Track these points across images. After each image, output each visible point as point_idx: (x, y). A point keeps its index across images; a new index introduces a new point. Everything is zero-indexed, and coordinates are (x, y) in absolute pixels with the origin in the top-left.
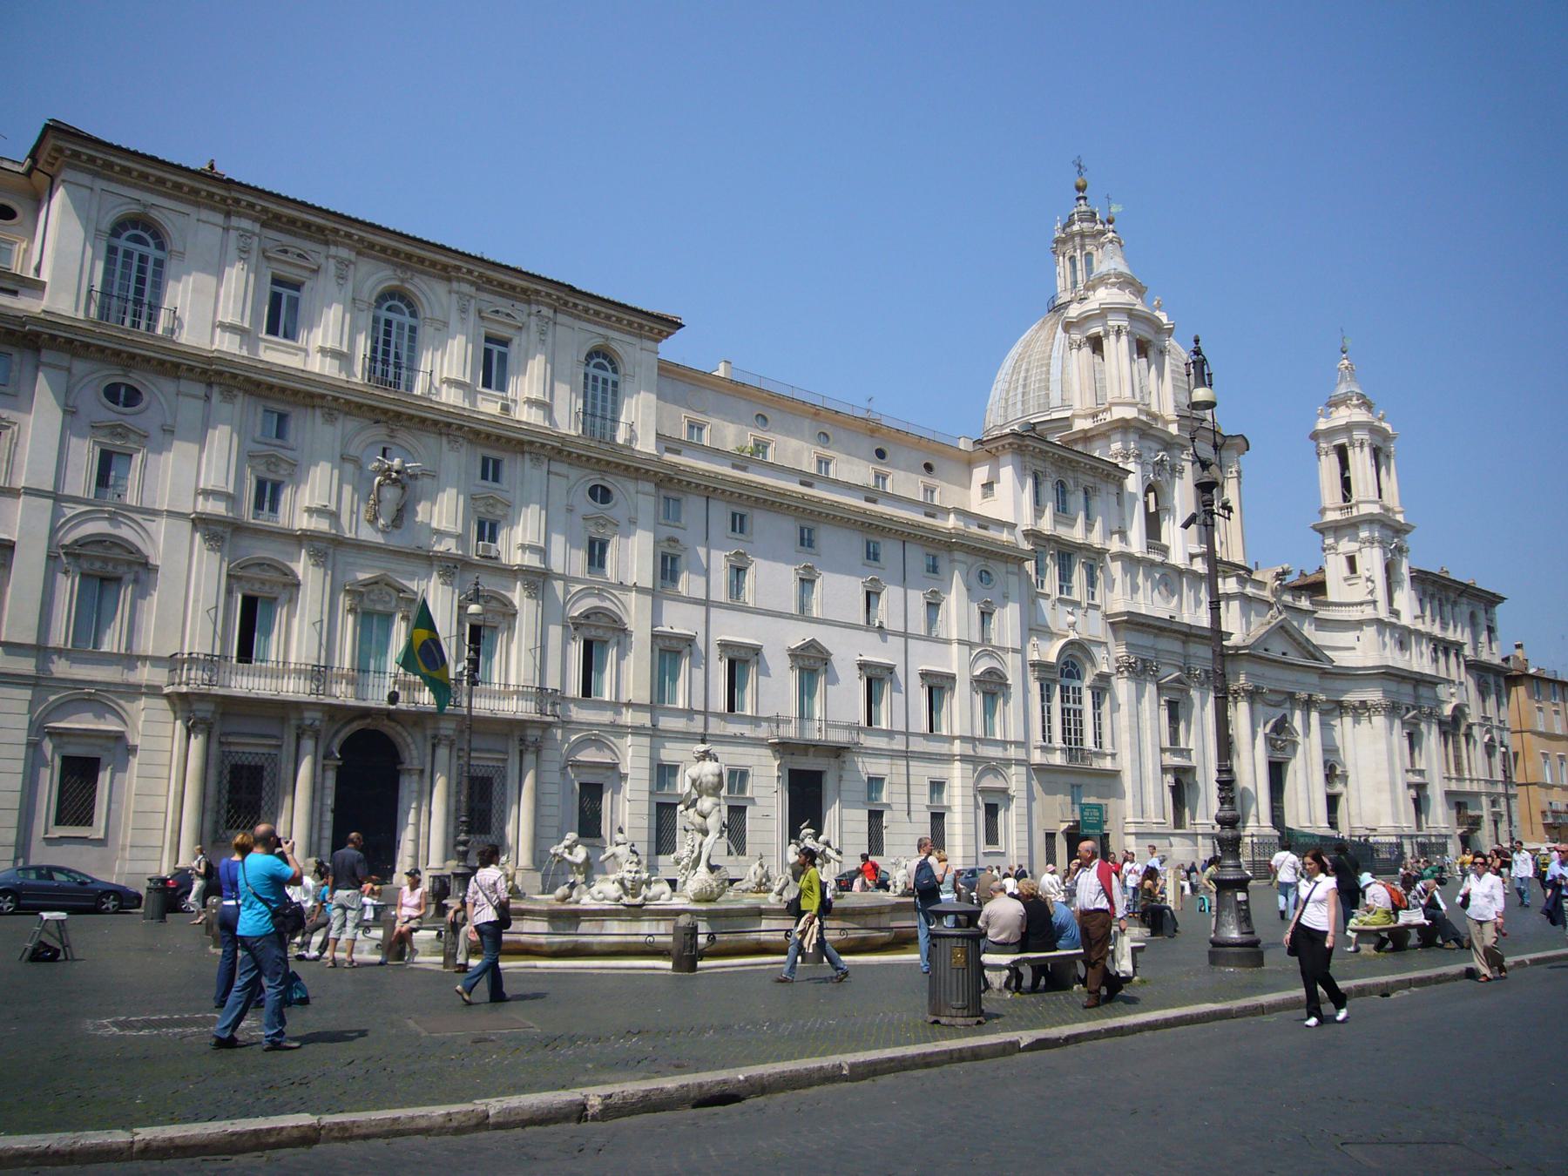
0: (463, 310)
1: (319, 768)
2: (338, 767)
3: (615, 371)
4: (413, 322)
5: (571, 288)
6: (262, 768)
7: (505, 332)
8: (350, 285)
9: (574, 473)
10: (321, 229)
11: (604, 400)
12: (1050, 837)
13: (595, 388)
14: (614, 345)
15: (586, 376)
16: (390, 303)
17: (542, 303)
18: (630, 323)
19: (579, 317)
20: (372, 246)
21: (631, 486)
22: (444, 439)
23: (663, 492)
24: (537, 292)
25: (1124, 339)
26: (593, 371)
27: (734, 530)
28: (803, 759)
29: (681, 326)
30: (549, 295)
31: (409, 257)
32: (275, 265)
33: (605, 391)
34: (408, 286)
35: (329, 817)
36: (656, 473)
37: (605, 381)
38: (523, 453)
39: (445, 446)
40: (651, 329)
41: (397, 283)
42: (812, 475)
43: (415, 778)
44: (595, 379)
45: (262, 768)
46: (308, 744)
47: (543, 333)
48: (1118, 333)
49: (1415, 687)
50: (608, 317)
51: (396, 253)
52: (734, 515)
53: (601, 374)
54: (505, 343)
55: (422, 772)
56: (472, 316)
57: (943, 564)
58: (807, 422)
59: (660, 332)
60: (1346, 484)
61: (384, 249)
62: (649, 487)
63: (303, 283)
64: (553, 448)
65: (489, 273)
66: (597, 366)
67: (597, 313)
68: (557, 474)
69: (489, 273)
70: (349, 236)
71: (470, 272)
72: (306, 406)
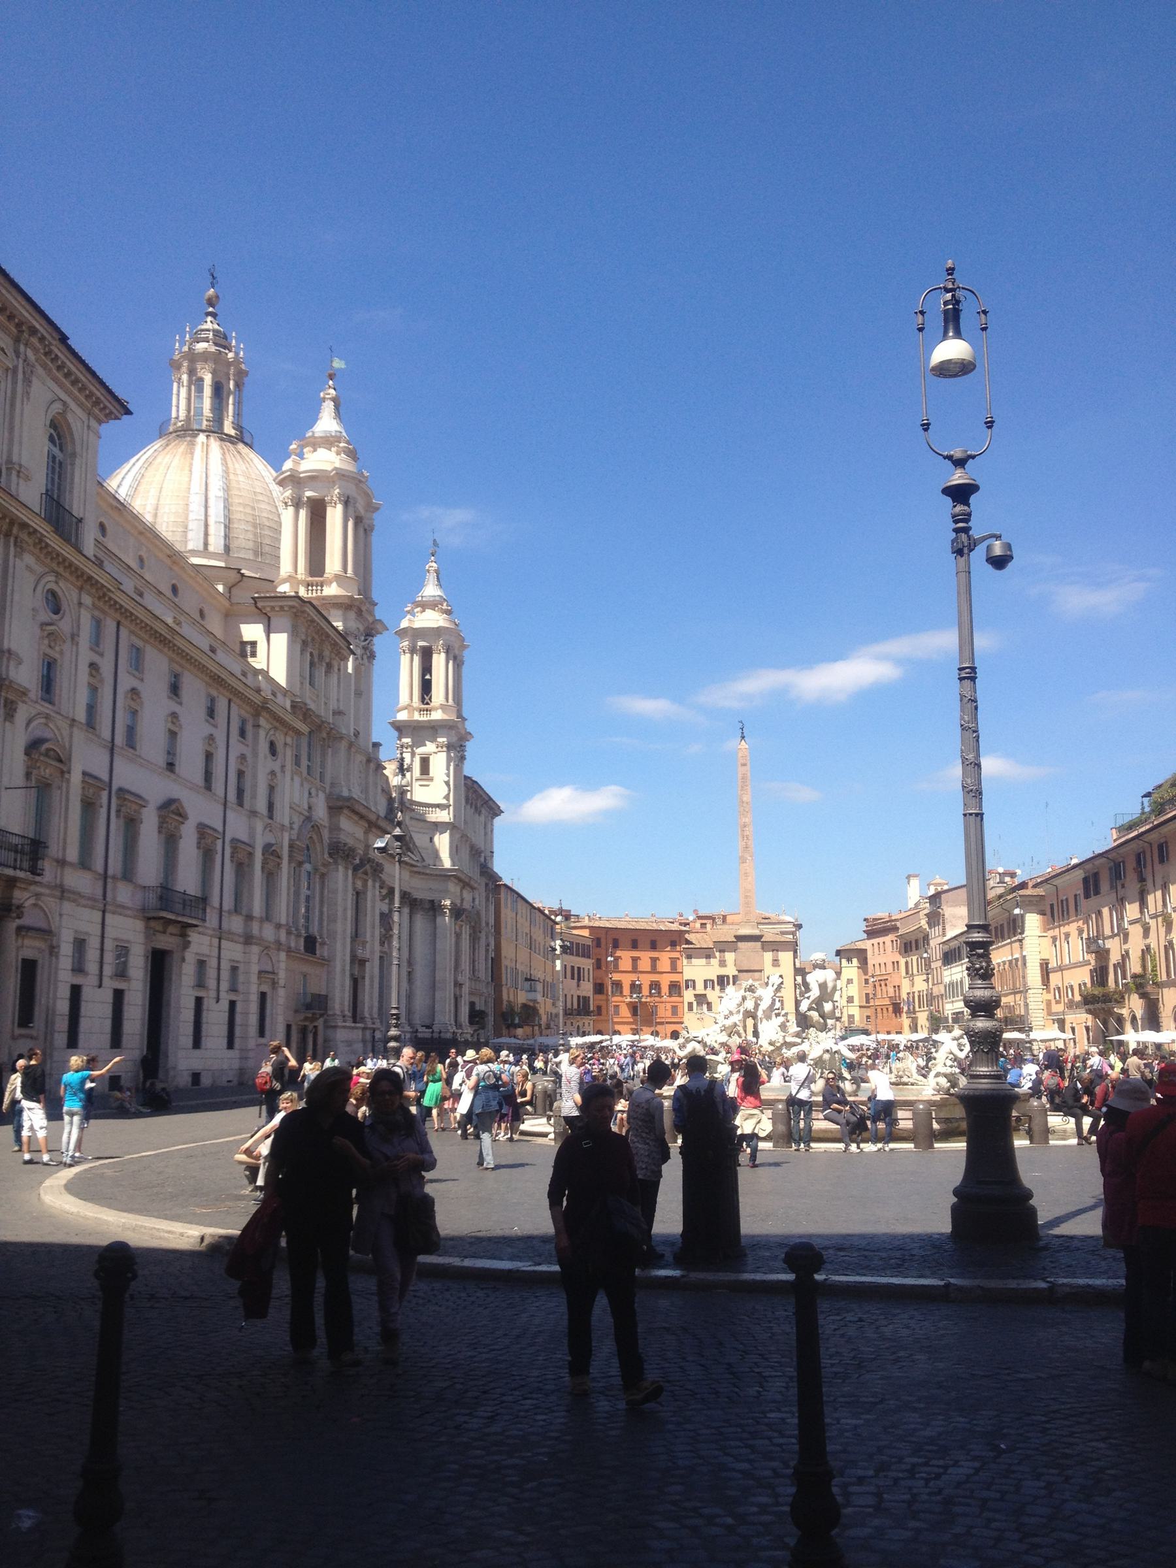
5: (64, 339)
12: (289, 1027)
14: (70, 417)
24: (33, 331)
28: (161, 937)
29: (128, 412)
30: (42, 339)
49: (463, 888)
60: (426, 687)
62: (87, 600)
67: (68, 375)
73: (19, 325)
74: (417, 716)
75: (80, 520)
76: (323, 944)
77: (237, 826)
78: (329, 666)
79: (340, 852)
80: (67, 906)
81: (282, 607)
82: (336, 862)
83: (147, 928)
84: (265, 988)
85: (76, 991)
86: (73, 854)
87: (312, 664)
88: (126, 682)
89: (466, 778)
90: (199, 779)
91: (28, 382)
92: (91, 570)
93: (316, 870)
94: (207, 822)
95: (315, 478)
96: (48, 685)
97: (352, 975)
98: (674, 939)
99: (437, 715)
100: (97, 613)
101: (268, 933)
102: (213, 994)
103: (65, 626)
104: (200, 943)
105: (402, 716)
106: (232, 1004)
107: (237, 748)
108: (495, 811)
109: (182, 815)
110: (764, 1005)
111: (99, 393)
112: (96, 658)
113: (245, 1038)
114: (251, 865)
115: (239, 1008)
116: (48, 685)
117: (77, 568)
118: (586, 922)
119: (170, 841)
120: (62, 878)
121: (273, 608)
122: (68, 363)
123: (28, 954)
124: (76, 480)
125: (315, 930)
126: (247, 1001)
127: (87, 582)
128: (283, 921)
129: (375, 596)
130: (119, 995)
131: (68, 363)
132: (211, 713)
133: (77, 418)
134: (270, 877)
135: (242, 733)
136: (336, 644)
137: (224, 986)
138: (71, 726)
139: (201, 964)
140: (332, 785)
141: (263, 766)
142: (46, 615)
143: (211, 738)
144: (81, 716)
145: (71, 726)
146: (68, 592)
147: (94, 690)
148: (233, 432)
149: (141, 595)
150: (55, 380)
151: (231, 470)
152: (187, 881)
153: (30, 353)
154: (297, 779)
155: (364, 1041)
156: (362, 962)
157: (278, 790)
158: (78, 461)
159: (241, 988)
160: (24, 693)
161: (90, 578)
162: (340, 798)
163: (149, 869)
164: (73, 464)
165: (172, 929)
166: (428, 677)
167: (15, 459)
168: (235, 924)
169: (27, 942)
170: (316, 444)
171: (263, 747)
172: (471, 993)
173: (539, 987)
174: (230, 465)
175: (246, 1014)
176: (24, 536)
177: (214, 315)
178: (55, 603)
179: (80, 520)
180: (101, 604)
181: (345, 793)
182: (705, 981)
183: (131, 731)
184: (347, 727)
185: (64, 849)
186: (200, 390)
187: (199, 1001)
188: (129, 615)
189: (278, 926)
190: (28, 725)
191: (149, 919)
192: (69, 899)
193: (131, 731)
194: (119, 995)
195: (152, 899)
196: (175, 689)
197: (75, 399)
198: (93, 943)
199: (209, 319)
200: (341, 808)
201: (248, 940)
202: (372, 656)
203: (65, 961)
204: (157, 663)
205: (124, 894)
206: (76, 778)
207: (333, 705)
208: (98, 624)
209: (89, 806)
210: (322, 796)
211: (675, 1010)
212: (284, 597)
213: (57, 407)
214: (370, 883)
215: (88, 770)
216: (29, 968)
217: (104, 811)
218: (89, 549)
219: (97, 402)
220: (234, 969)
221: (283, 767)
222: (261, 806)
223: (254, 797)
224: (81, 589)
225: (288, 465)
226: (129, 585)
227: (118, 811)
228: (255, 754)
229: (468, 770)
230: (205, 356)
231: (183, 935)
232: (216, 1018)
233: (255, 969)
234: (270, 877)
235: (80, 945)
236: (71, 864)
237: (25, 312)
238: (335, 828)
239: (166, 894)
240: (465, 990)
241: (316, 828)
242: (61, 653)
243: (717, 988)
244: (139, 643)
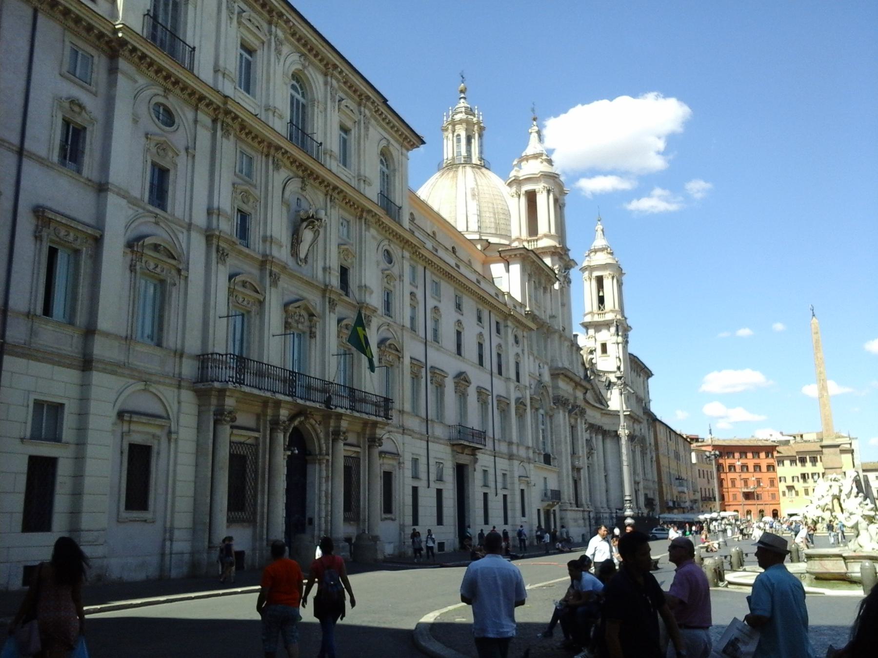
5: (385, 101)
7: (349, 124)
12: (539, 510)
14: (391, 148)
24: (368, 98)
25: (551, 196)
29: (423, 143)
30: (373, 102)
38: (361, 218)
41: (300, 67)
48: (549, 191)
60: (601, 300)
62: (407, 254)
70: (287, 21)
73: (360, 96)
74: (596, 318)
75: (400, 208)
76: (555, 458)
77: (499, 387)
78: (545, 289)
79: (560, 402)
80: (407, 438)
81: (515, 255)
82: (558, 408)
83: (453, 451)
84: (523, 487)
85: (415, 490)
86: (408, 407)
87: (535, 288)
88: (431, 303)
89: (630, 354)
90: (476, 360)
92: (407, 236)
93: (547, 413)
94: (481, 385)
95: (529, 180)
96: (388, 305)
97: (573, 477)
98: (769, 450)
99: (609, 316)
100: (412, 262)
101: (522, 452)
102: (493, 491)
103: (395, 270)
104: (484, 460)
105: (588, 319)
106: (505, 496)
107: (496, 340)
108: (649, 374)
109: (467, 381)
110: (846, 490)
111: (407, 133)
112: (414, 290)
113: (514, 517)
115: (509, 499)
116: (388, 305)
117: (400, 236)
118: (709, 442)
119: (462, 396)
123: (387, 468)
124: (397, 184)
125: (549, 450)
126: (513, 494)
127: (406, 243)
128: (530, 445)
129: (569, 245)
130: (439, 492)
132: (480, 319)
133: (395, 149)
134: (521, 416)
135: (498, 331)
136: (548, 275)
137: (500, 486)
138: (402, 330)
139: (485, 471)
140: (552, 361)
141: (511, 351)
142: (384, 265)
143: (481, 334)
144: (408, 324)
146: (396, 250)
147: (413, 308)
148: (479, 163)
149: (436, 251)
150: (381, 126)
151: (479, 184)
152: (474, 421)
153: (367, 112)
154: (531, 358)
155: (584, 519)
156: (579, 470)
157: (521, 365)
158: (397, 173)
159: (509, 486)
160: (375, 311)
161: (408, 241)
162: (557, 368)
163: (451, 415)
164: (394, 176)
165: (466, 451)
166: (601, 294)
167: (362, 173)
168: (503, 448)
169: (386, 461)
170: (527, 158)
171: (511, 339)
172: (644, 488)
173: (685, 484)
174: (478, 181)
175: (513, 502)
176: (369, 218)
177: (465, 98)
178: (389, 257)
179: (400, 208)
180: (415, 257)
181: (560, 365)
182: (793, 477)
183: (435, 331)
184: (558, 325)
186: (459, 141)
187: (485, 495)
188: (430, 263)
189: (528, 448)
190: (378, 330)
191: (453, 445)
192: (406, 434)
193: (435, 331)
194: (439, 492)
195: (454, 433)
196: (459, 307)
197: (393, 137)
198: (423, 461)
199: (462, 100)
200: (558, 374)
201: (511, 457)
202: (569, 282)
203: (408, 473)
204: (448, 290)
206: (407, 361)
207: (549, 312)
208: (413, 269)
209: (415, 377)
210: (546, 367)
211: (774, 496)
212: (517, 249)
213: (384, 143)
214: (579, 420)
215: (413, 356)
216: (388, 477)
217: (423, 380)
218: (406, 223)
219: (406, 138)
220: (504, 475)
221: (523, 350)
222: (513, 376)
223: (508, 369)
224: (403, 248)
225: (513, 174)
226: (429, 245)
227: (431, 380)
228: (507, 343)
229: (631, 349)
230: (461, 122)
231: (474, 455)
232: (496, 505)
233: (516, 475)
234: (521, 416)
235: (415, 461)
236: (408, 413)
237: (363, 88)
238: (556, 387)
239: (462, 430)
240: (641, 486)
241: (545, 387)
242: (394, 286)
243: (801, 481)
244: (437, 279)
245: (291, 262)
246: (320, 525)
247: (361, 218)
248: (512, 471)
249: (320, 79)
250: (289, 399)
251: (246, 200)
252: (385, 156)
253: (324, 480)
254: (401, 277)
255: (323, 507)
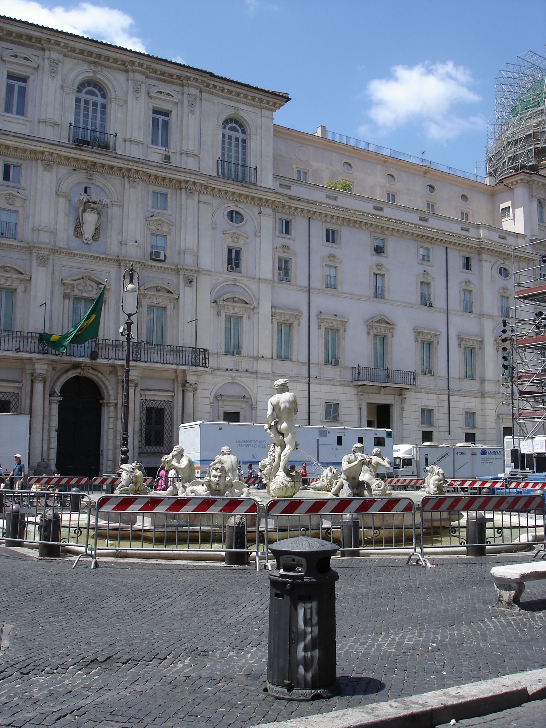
0: (137, 91)
1: (47, 402)
2: (60, 401)
3: (244, 132)
4: (103, 101)
5: (211, 75)
6: (9, 402)
7: (166, 107)
8: (59, 78)
9: (216, 202)
10: (39, 40)
11: (237, 152)
13: (230, 144)
14: (243, 114)
15: (224, 136)
16: (91, 88)
17: (192, 86)
18: (253, 99)
19: (217, 95)
20: (73, 50)
21: (256, 211)
22: (126, 180)
23: (278, 215)
24: (188, 78)
26: (228, 132)
27: (328, 240)
28: (377, 396)
29: (289, 99)
30: (197, 80)
31: (99, 56)
32: (8, 65)
33: (237, 146)
34: (99, 76)
35: (54, 435)
36: (273, 202)
37: (237, 139)
39: (127, 185)
40: (268, 102)
41: (91, 74)
42: (382, 202)
43: (112, 409)
44: (230, 137)
45: (9, 402)
46: (39, 387)
47: (192, 105)
50: (238, 95)
51: (90, 54)
52: (328, 231)
53: (234, 134)
54: (167, 114)
55: (116, 404)
56: (143, 96)
57: (474, 263)
58: (379, 167)
59: (274, 104)
61: (82, 52)
62: (269, 211)
63: (28, 77)
64: (201, 185)
65: (154, 65)
66: (232, 129)
67: (230, 92)
68: (204, 202)
69: (154, 65)
70: (57, 43)
71: (141, 65)
72: (32, 160)
81: (517, 181)
83: (358, 392)
91: (192, 105)
114: (482, 348)
120: (257, 367)
121: (512, 183)
122: (225, 86)
124: (253, 146)
131: (225, 86)
145: (259, 283)
159: (478, 424)
161: (260, 199)
168: (473, 385)
179: (256, 169)
185: (258, 351)
201: (483, 395)
205: (330, 372)
206: (265, 309)
227: (319, 327)
228: (481, 278)
231: (400, 395)
237: (176, 71)
245: (75, 243)
246: (107, 456)
247: (181, 189)
248: (483, 409)
249: (121, 77)
250: (40, 356)
251: (10, 201)
252: (234, 123)
253: (111, 420)
254: (257, 234)
255: (111, 441)
